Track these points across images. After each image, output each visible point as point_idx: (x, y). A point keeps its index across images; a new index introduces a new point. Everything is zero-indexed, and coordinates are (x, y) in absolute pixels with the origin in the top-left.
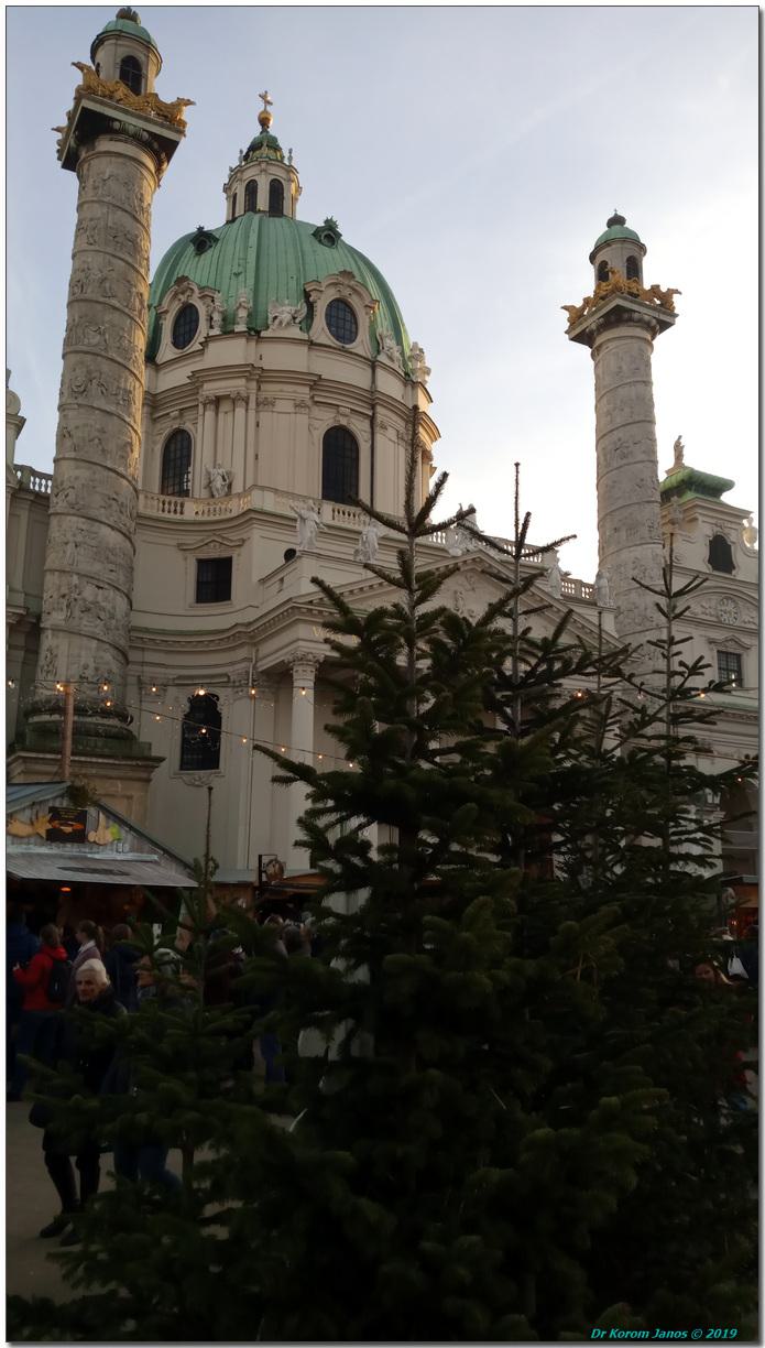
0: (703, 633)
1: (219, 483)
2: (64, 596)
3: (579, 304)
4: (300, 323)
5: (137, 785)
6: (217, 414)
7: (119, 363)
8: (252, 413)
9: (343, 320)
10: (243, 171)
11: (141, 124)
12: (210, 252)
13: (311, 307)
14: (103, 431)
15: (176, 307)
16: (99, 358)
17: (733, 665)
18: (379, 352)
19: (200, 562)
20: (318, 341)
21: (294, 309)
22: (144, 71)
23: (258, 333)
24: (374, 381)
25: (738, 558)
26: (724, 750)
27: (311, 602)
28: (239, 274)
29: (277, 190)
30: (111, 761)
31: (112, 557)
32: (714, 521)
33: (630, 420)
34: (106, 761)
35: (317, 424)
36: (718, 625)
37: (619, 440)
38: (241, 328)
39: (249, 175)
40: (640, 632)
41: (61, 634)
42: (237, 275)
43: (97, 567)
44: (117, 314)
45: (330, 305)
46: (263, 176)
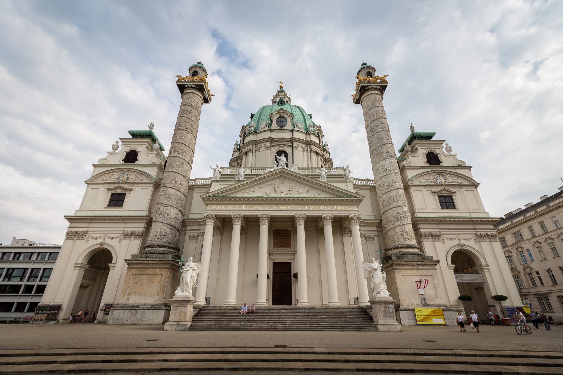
0: (429, 189)
3: (355, 93)
5: (165, 270)
7: (180, 143)
8: (254, 154)
10: (273, 100)
13: (271, 121)
15: (243, 133)
16: (175, 143)
17: (448, 200)
18: (295, 127)
20: (274, 129)
22: (198, 73)
23: (257, 132)
24: (293, 136)
25: (442, 158)
26: (449, 237)
27: (209, 196)
30: (155, 262)
32: (426, 147)
33: (374, 119)
34: (153, 262)
35: (273, 151)
36: (436, 185)
37: (371, 127)
40: (388, 192)
43: (166, 200)
44: (182, 131)
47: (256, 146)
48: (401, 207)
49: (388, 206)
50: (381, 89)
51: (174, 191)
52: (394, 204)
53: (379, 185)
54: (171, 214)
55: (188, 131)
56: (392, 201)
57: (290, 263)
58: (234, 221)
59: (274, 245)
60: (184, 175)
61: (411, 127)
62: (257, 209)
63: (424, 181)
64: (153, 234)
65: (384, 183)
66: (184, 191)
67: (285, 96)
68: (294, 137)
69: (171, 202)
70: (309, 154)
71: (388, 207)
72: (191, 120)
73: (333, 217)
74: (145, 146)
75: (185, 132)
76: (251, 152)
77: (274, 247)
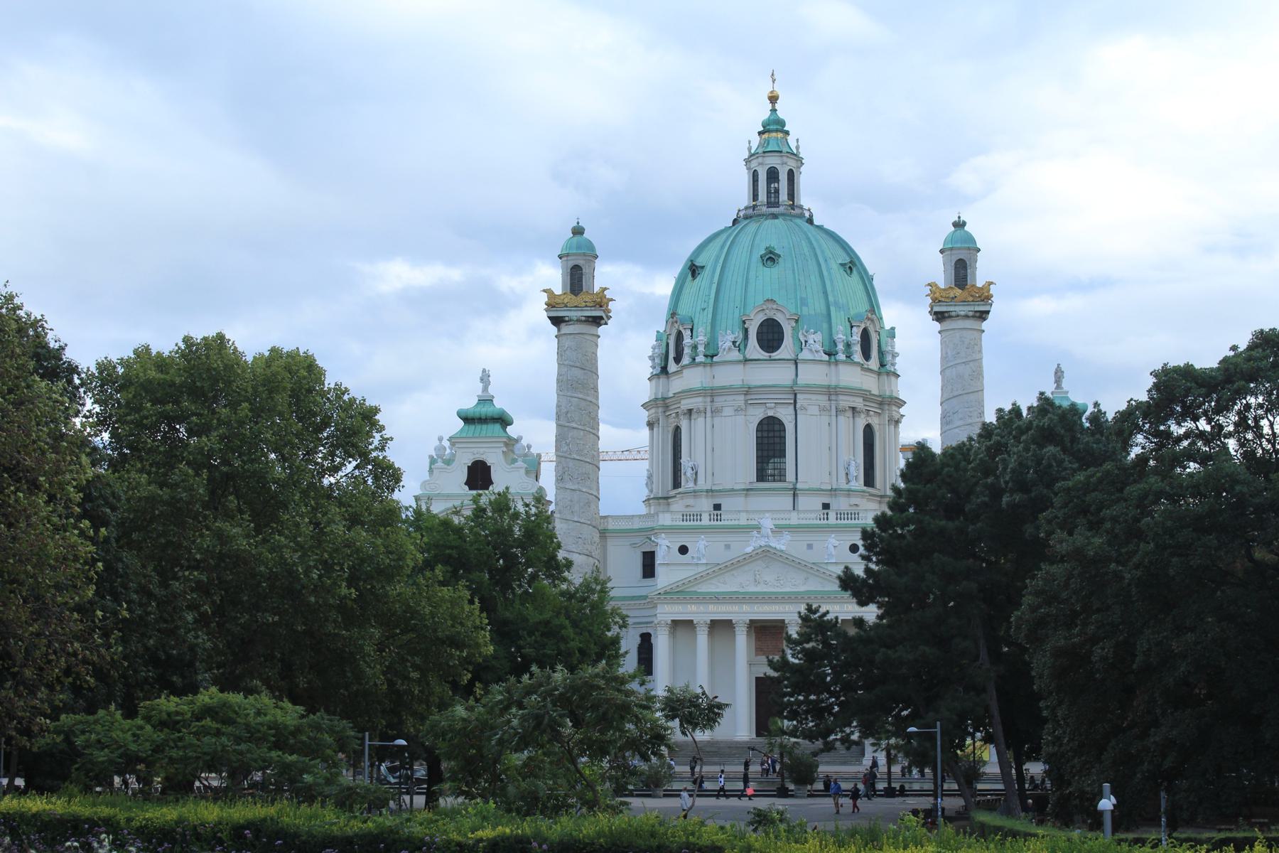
1: (689, 473)
6: (690, 420)
8: (709, 419)
9: (771, 336)
11: (579, 314)
12: (698, 279)
13: (746, 330)
14: (571, 501)
15: (674, 332)
18: (802, 349)
19: (645, 554)
21: (733, 336)
22: (584, 270)
23: (712, 357)
24: (797, 375)
28: (704, 309)
29: (773, 175)
38: (700, 358)
39: (754, 164)
42: (704, 309)
45: (761, 325)
47: (712, 401)
50: (978, 314)
55: (587, 429)
60: (594, 523)
61: (1056, 373)
67: (785, 159)
70: (834, 418)
72: (588, 403)
74: (499, 451)
75: (582, 433)
76: (703, 414)
77: (756, 655)
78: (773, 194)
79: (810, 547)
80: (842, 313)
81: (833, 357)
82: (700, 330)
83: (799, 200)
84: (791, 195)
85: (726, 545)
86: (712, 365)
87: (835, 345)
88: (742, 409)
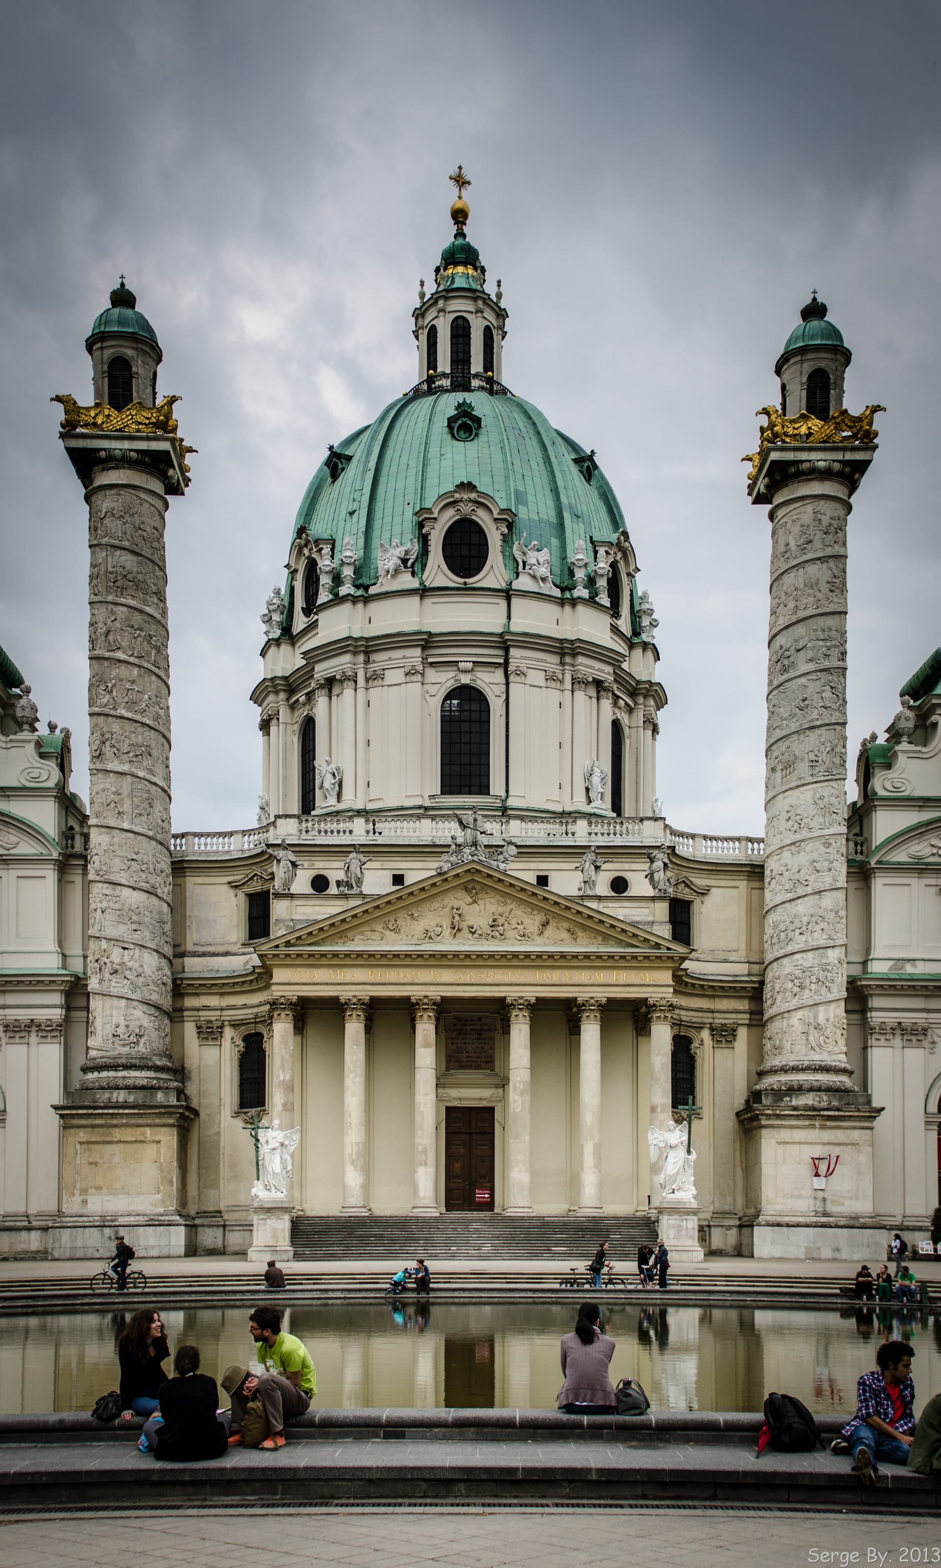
0: (933, 881)
2: (97, 961)
4: (413, 566)
19: (250, 896)
20: (432, 586)
23: (366, 588)
24: (509, 617)
29: (461, 330)
31: (135, 918)
40: (790, 901)
41: (97, 996)
42: (352, 513)
46: (441, 319)
48: (817, 952)
49: (783, 944)
51: (143, 896)
52: (800, 942)
53: (772, 871)
54: (147, 971)
56: (798, 931)
57: (493, 1108)
58: (348, 1013)
59: (448, 1062)
62: (406, 980)
63: (928, 851)
64: (106, 1032)
65: (784, 869)
66: (166, 890)
67: (480, 303)
68: (513, 628)
69: (139, 932)
71: (782, 948)
73: (604, 1001)
78: (461, 357)
79: (543, 881)
80: (581, 525)
81: (567, 595)
82: (346, 540)
83: (499, 373)
84: (489, 363)
85: (394, 875)
86: (367, 600)
87: (571, 573)
88: (417, 672)
